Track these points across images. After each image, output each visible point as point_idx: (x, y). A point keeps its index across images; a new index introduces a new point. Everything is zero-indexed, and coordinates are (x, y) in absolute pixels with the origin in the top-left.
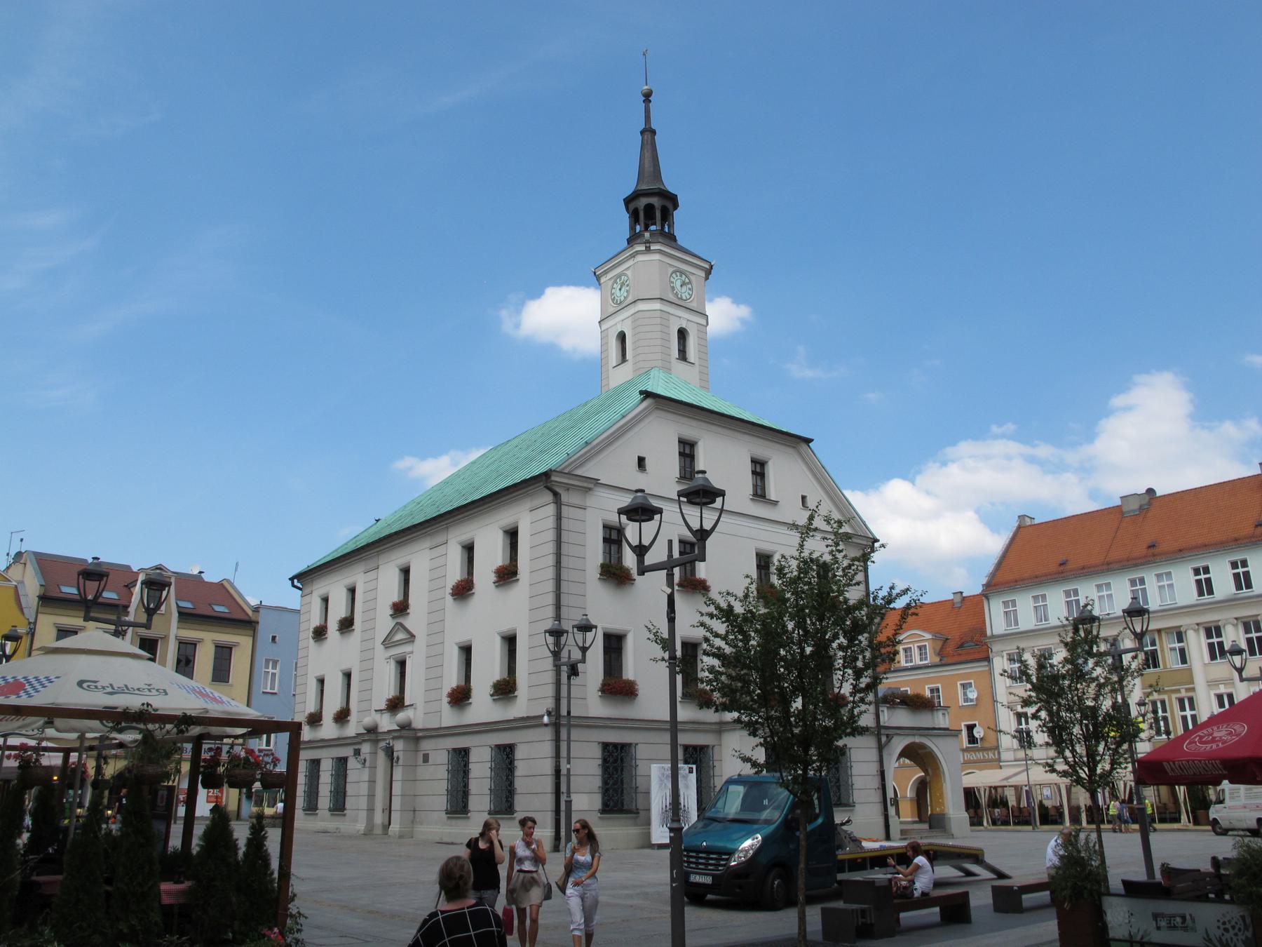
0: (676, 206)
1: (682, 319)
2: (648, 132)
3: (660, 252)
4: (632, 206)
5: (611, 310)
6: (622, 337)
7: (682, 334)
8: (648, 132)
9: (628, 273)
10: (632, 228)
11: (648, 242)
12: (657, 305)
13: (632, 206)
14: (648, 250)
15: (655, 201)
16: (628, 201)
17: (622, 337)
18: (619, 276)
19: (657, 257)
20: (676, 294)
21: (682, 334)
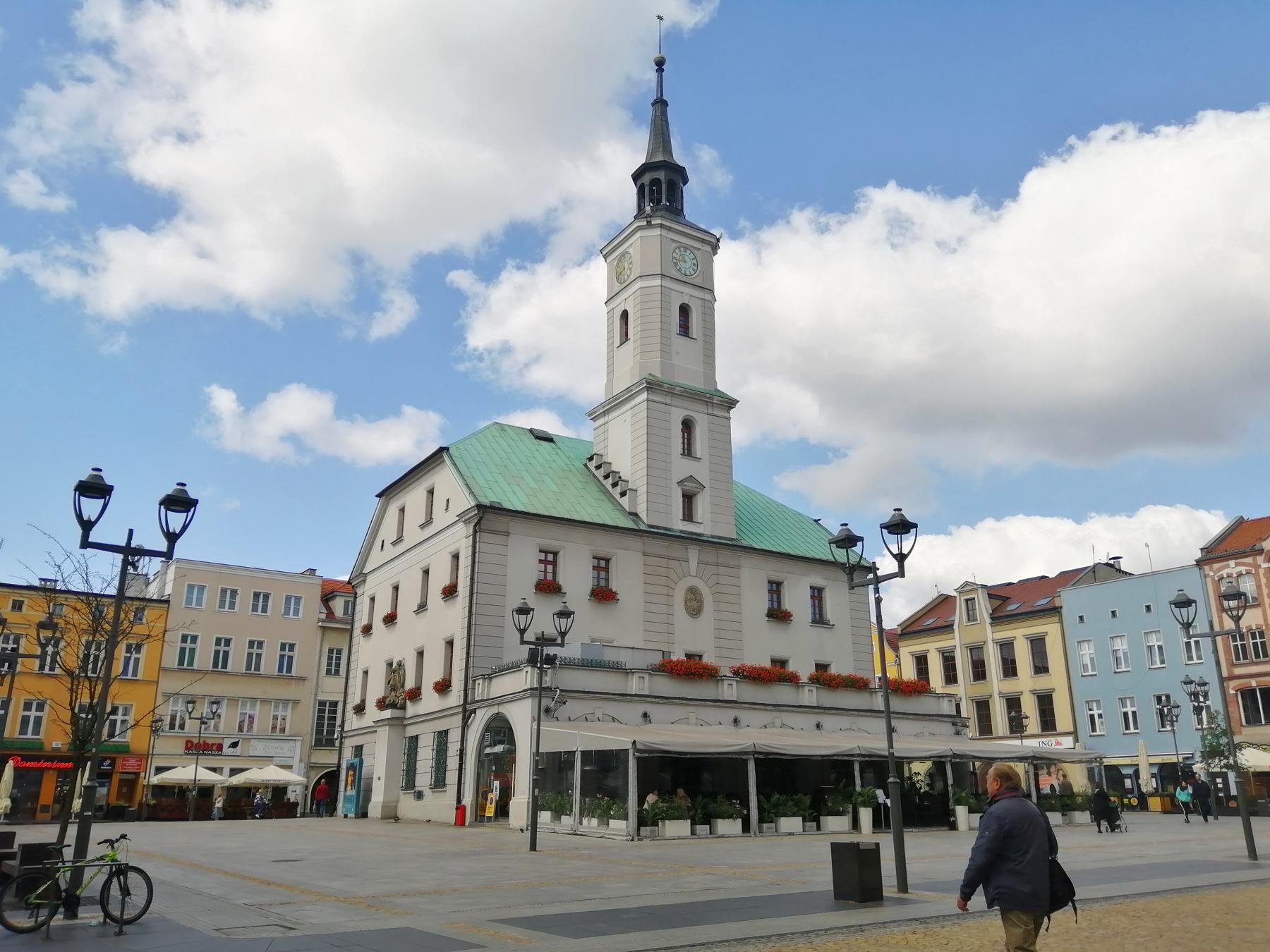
0: (685, 181)
1: (686, 295)
2: (661, 103)
3: (661, 226)
4: (639, 183)
5: (617, 289)
6: (625, 315)
7: (684, 310)
8: (661, 103)
9: (631, 250)
10: (640, 208)
11: (649, 216)
12: (658, 282)
13: (639, 183)
14: (649, 225)
15: (661, 175)
16: (636, 177)
17: (625, 315)
18: (623, 255)
19: (658, 232)
20: (680, 270)
21: (684, 310)
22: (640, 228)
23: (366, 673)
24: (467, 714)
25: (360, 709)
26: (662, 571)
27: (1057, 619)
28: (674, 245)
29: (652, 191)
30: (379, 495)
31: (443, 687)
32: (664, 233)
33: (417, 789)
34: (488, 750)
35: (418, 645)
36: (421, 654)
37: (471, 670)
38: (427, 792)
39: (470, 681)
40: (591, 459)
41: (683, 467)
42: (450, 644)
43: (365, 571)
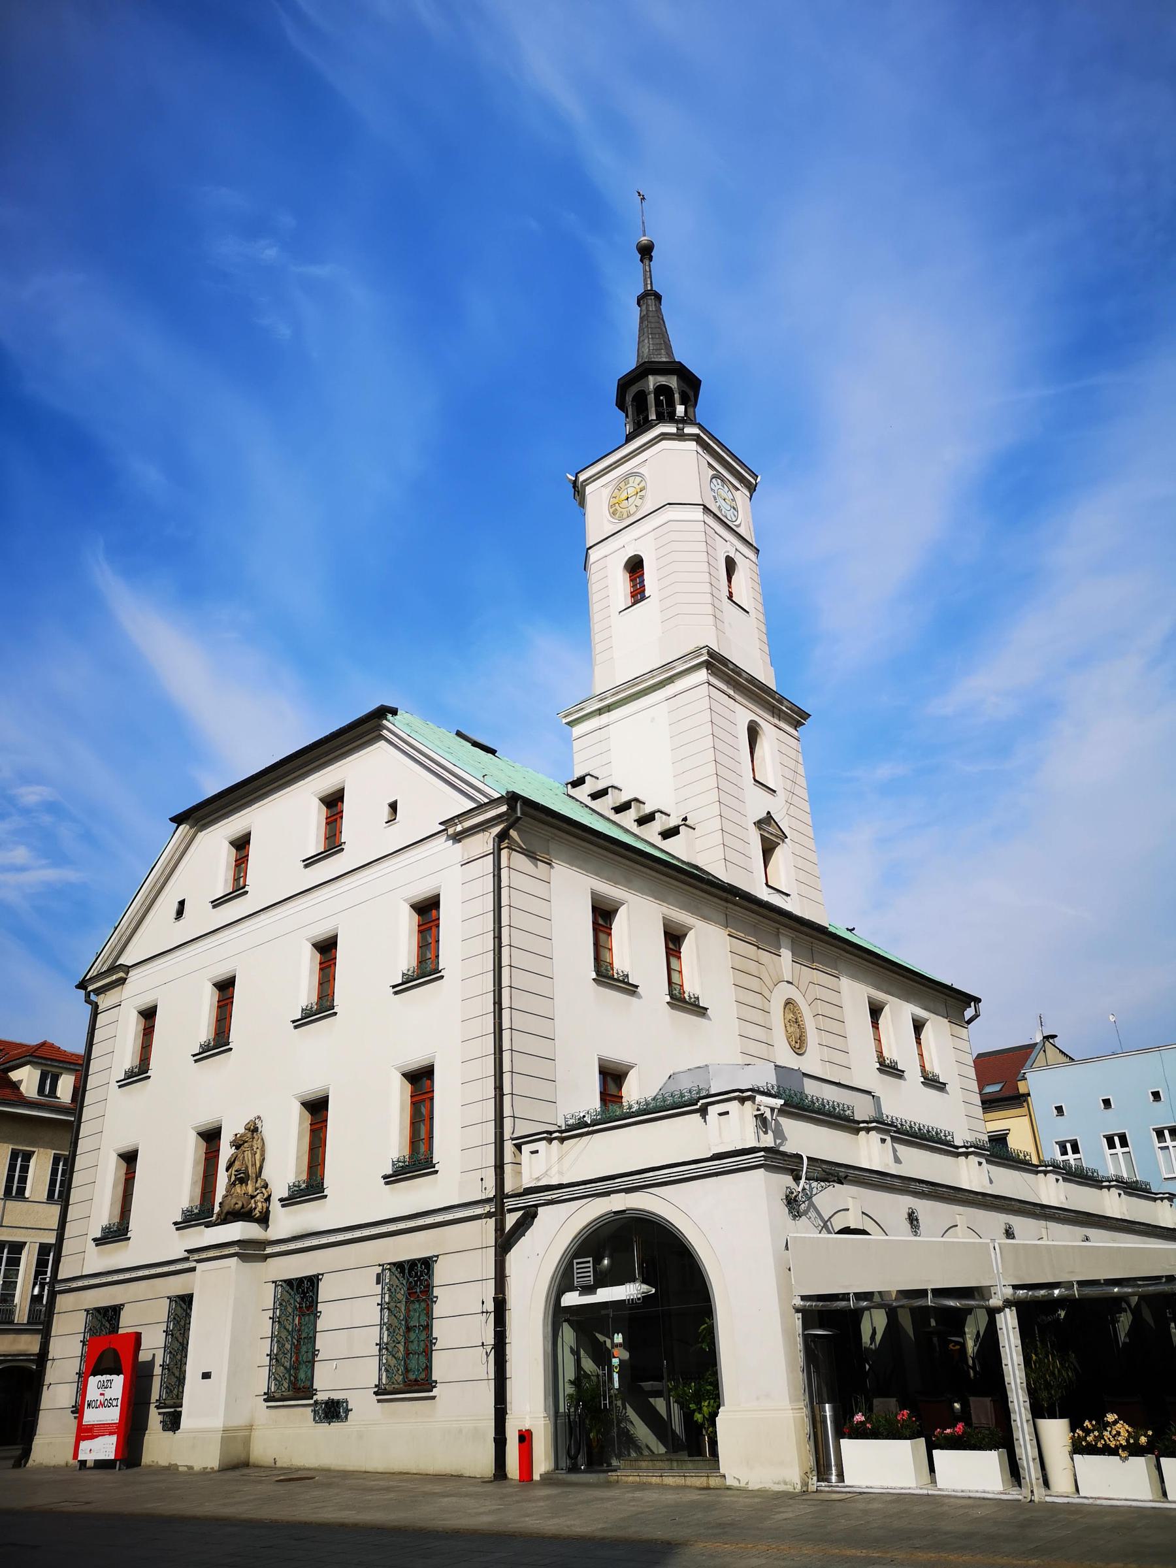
13: (633, 390)
15: (673, 382)
18: (626, 478)
19: (693, 445)
22: (664, 436)
23: (130, 1158)
24: (509, 1216)
25: (117, 1233)
26: (752, 967)
27: (1024, 1111)
28: (711, 473)
29: (658, 403)
30: (173, 820)
31: (417, 1162)
32: (700, 450)
33: (321, 1397)
34: (571, 1299)
35: (311, 1087)
36: (317, 1108)
37: (508, 1123)
38: (363, 1405)
39: (509, 1147)
40: (579, 782)
41: (757, 805)
42: (421, 1079)
43: (126, 959)
